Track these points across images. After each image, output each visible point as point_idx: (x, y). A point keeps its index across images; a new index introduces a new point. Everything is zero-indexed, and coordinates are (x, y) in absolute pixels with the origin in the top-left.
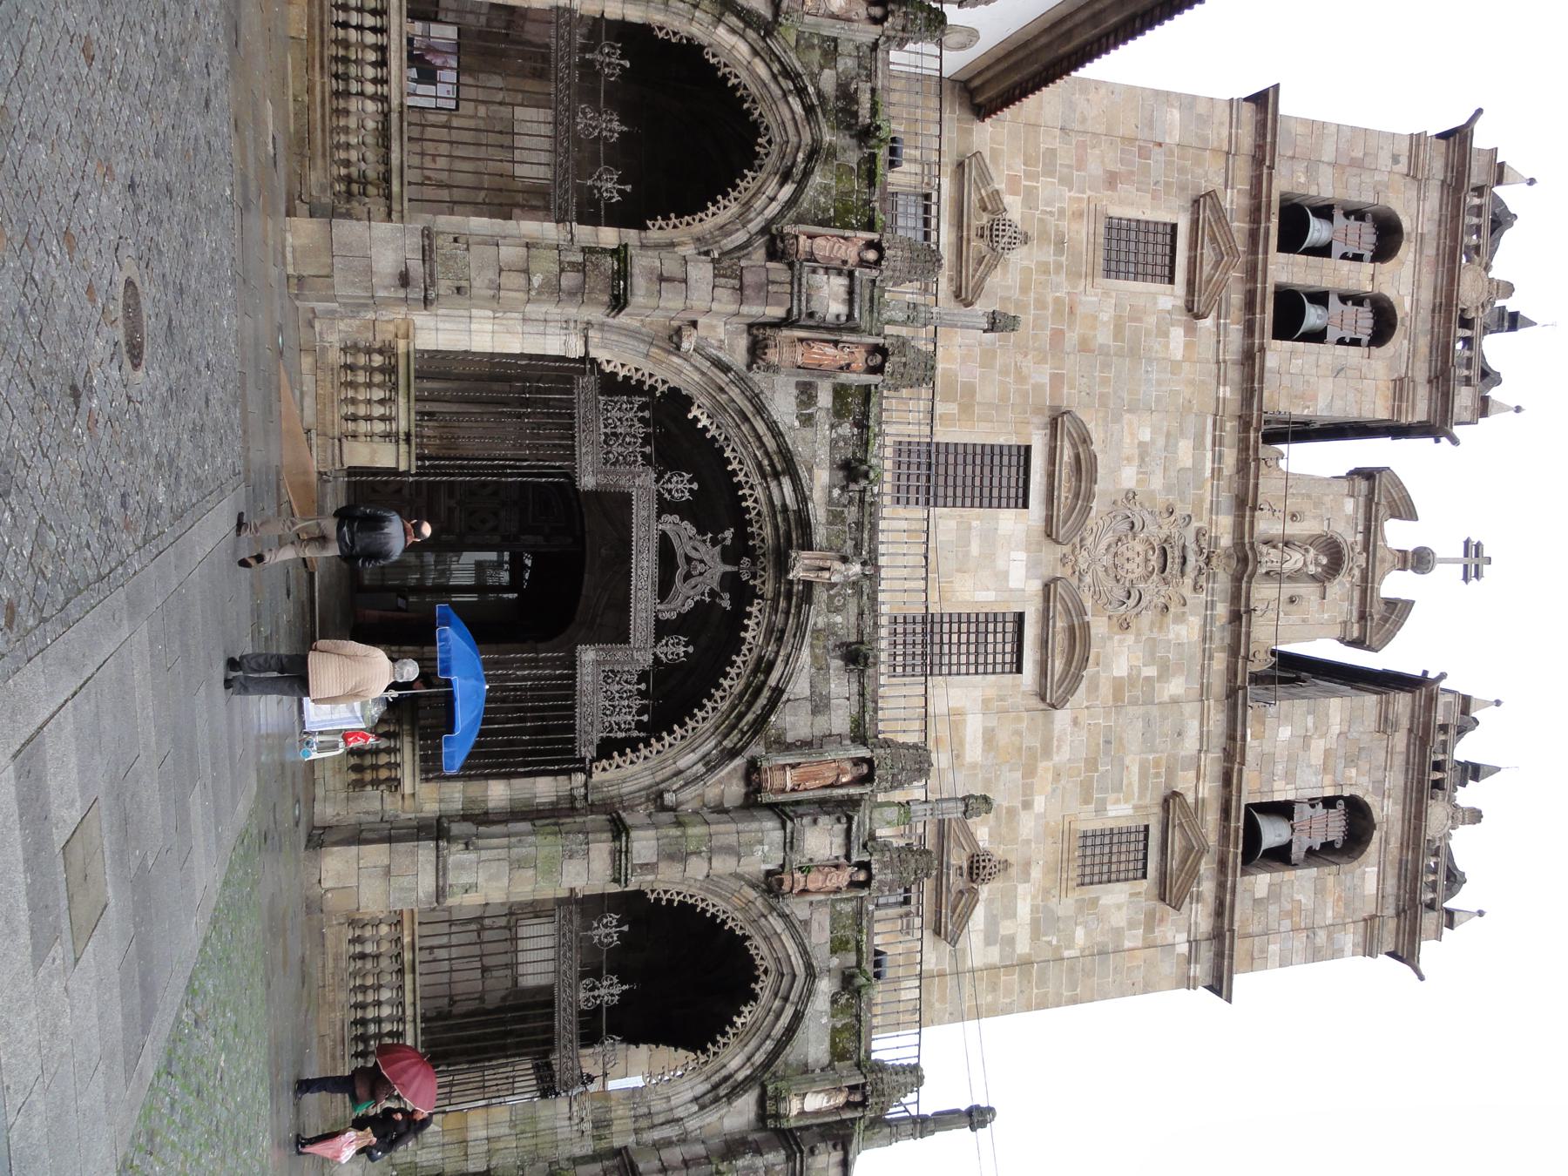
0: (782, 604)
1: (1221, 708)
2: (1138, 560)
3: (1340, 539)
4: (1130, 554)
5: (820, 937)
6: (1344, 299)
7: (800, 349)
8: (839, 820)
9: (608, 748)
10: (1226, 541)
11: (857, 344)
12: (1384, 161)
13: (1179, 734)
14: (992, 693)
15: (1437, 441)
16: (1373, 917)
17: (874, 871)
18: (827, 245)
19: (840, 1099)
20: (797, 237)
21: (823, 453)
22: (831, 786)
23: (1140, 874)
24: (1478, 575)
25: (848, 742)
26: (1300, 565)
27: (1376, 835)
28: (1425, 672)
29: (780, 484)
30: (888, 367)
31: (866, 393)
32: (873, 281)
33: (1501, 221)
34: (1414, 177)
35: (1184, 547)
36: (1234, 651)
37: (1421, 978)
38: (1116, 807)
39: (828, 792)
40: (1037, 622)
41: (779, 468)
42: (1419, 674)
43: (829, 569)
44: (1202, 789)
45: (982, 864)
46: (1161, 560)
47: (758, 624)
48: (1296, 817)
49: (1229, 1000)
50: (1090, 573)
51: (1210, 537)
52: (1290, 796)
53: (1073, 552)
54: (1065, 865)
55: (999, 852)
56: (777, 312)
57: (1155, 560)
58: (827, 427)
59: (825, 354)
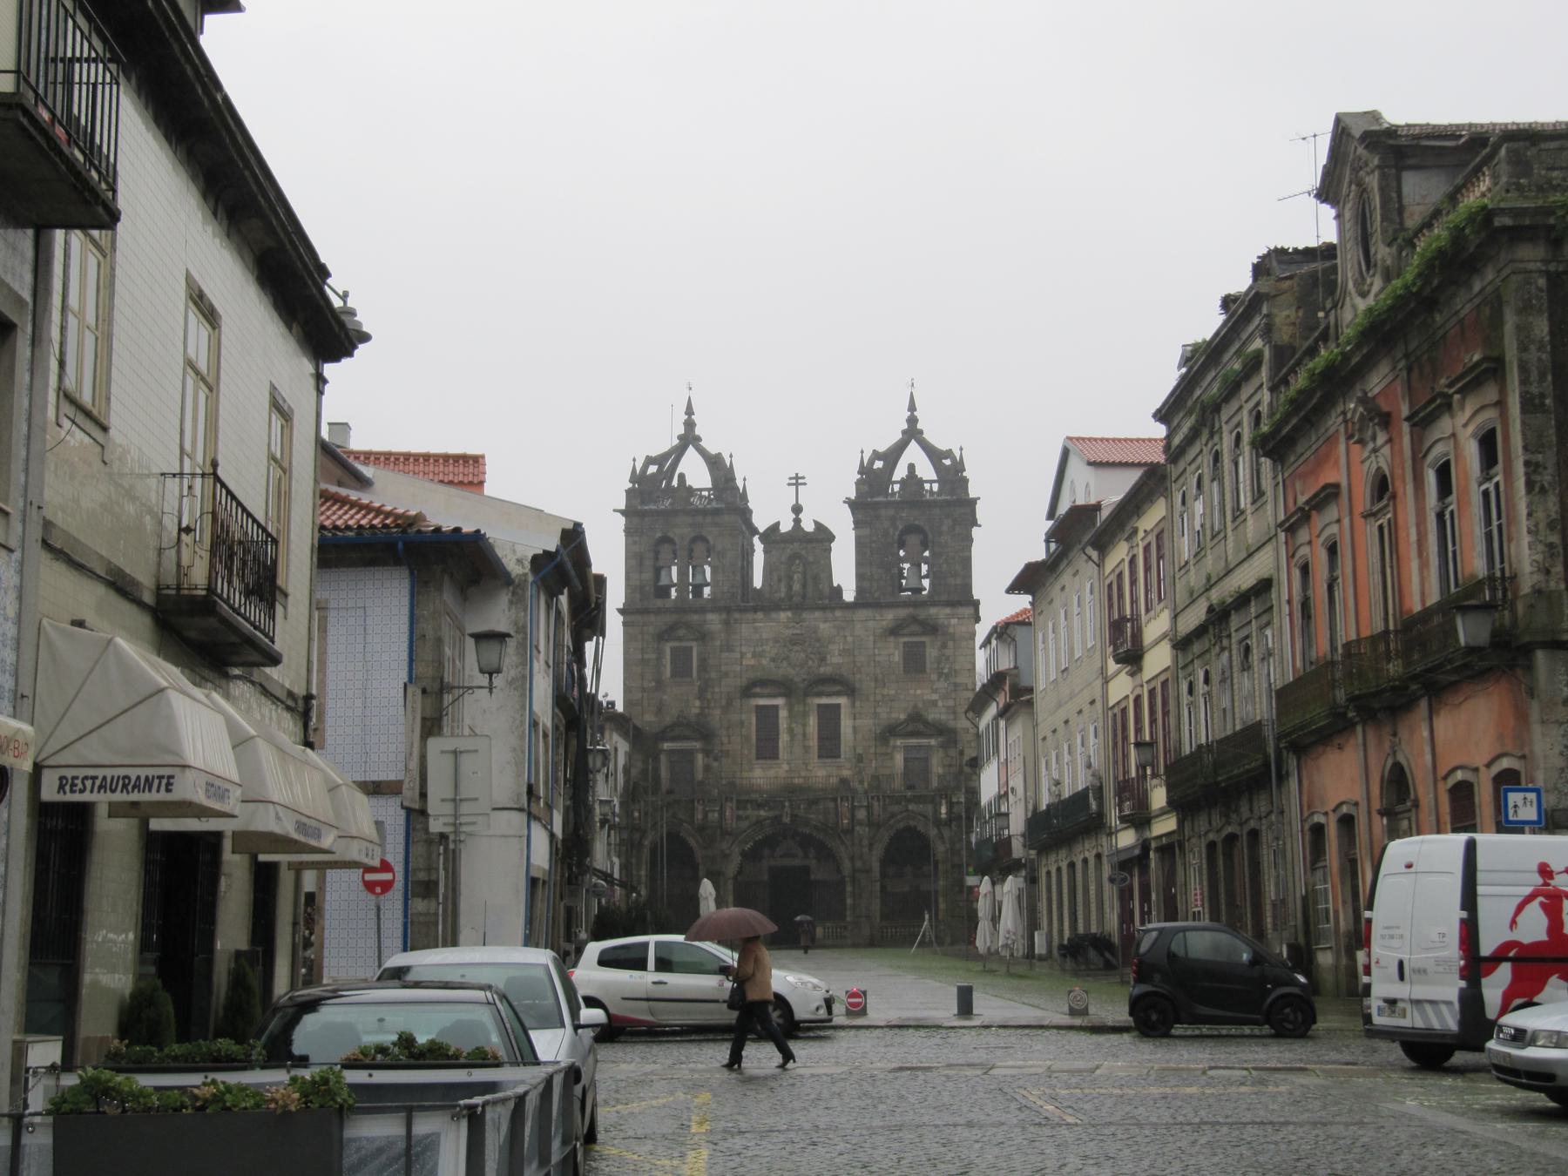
5: (896, 808)
9: (839, 871)
10: (789, 614)
18: (699, 816)
19: (944, 802)
24: (803, 478)
27: (917, 523)
31: (738, 801)
33: (649, 461)
36: (833, 609)
44: (890, 616)
57: (796, 648)
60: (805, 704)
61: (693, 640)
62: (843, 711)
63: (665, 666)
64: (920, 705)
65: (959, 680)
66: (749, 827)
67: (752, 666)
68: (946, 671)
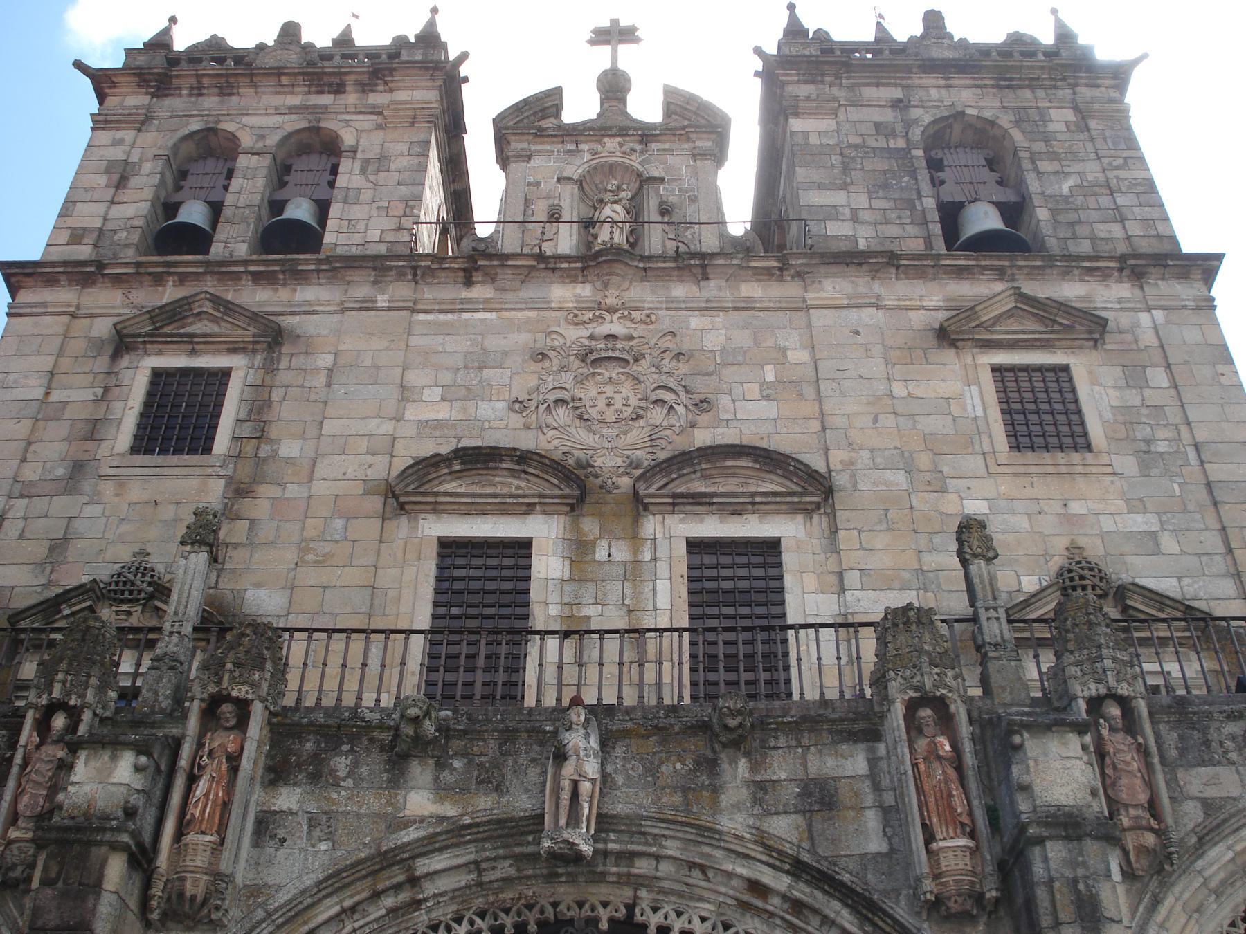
0: (642, 867)
1: (816, 286)
2: (610, 394)
3: (585, 166)
4: (601, 403)
6: (282, 184)
7: (191, 838)
8: (1019, 748)
10: (585, 291)
11: (200, 745)
12: (118, 154)
13: (857, 333)
14: (810, 581)
15: (466, 80)
16: (1076, 108)
17: (1103, 691)
20: (11, 842)
21: (374, 803)
22: (959, 768)
23: (1063, 375)
25: (881, 749)
26: (618, 208)
28: (757, 74)
29: (430, 875)
30: (239, 691)
32: (103, 720)
34: (143, 123)
35: (592, 337)
37: (1144, 57)
38: (969, 408)
39: (970, 774)
40: (702, 521)
41: (401, 878)
42: (759, 81)
43: (575, 784)
45: (1077, 581)
46: (610, 365)
47: (679, 914)
48: (957, 199)
49: (1219, 257)
50: (629, 453)
51: (580, 309)
52: (930, 203)
53: (596, 476)
54: (1063, 469)
55: (1057, 562)
56: (115, 869)
57: (611, 371)
58: (334, 795)
59: (207, 795)
60: (635, 538)
61: (234, 350)
62: (789, 559)
63: (119, 422)
64: (1094, 550)
65: (1217, 471)
66: (334, 882)
67: (438, 424)
68: (1162, 447)
